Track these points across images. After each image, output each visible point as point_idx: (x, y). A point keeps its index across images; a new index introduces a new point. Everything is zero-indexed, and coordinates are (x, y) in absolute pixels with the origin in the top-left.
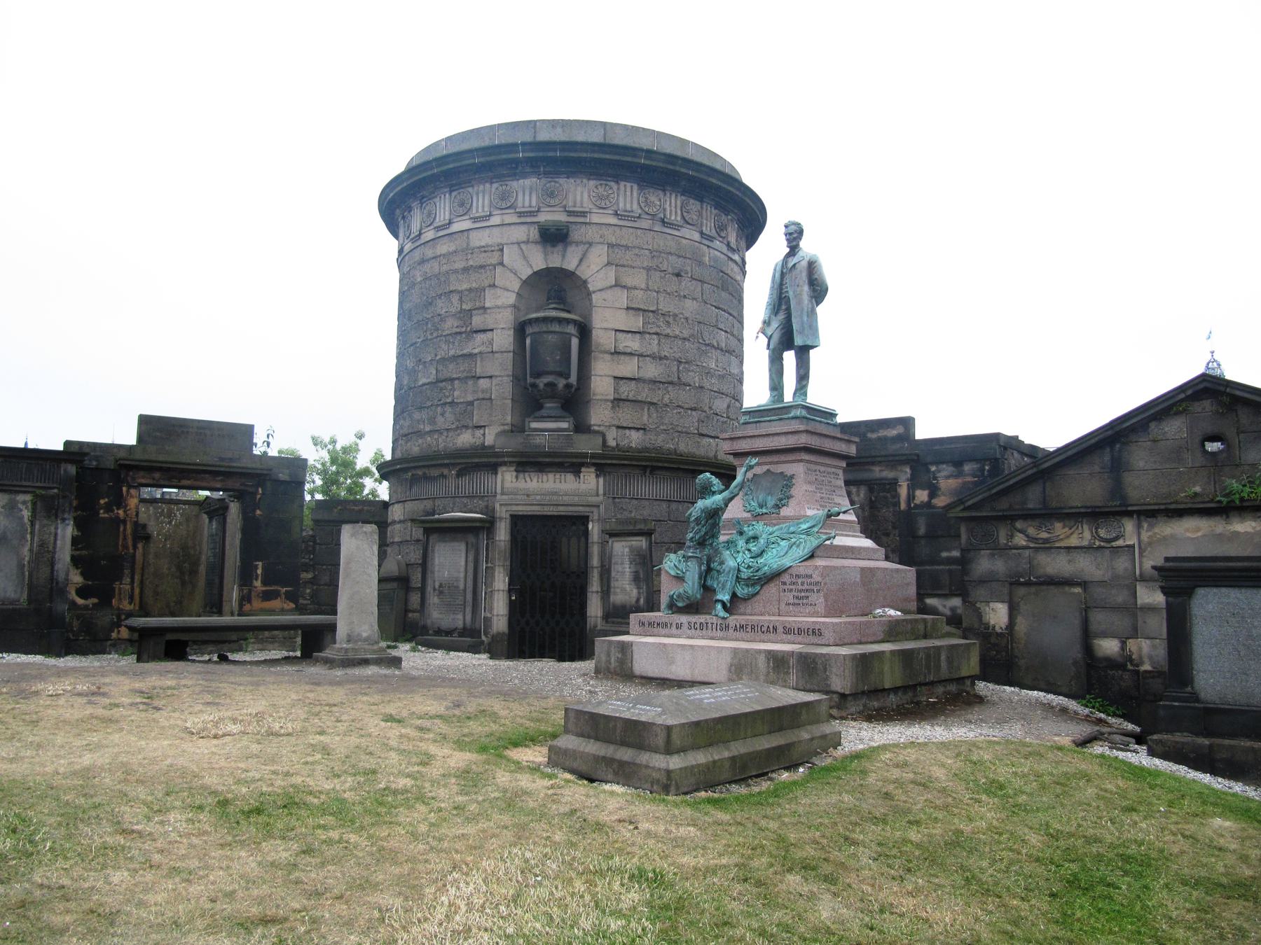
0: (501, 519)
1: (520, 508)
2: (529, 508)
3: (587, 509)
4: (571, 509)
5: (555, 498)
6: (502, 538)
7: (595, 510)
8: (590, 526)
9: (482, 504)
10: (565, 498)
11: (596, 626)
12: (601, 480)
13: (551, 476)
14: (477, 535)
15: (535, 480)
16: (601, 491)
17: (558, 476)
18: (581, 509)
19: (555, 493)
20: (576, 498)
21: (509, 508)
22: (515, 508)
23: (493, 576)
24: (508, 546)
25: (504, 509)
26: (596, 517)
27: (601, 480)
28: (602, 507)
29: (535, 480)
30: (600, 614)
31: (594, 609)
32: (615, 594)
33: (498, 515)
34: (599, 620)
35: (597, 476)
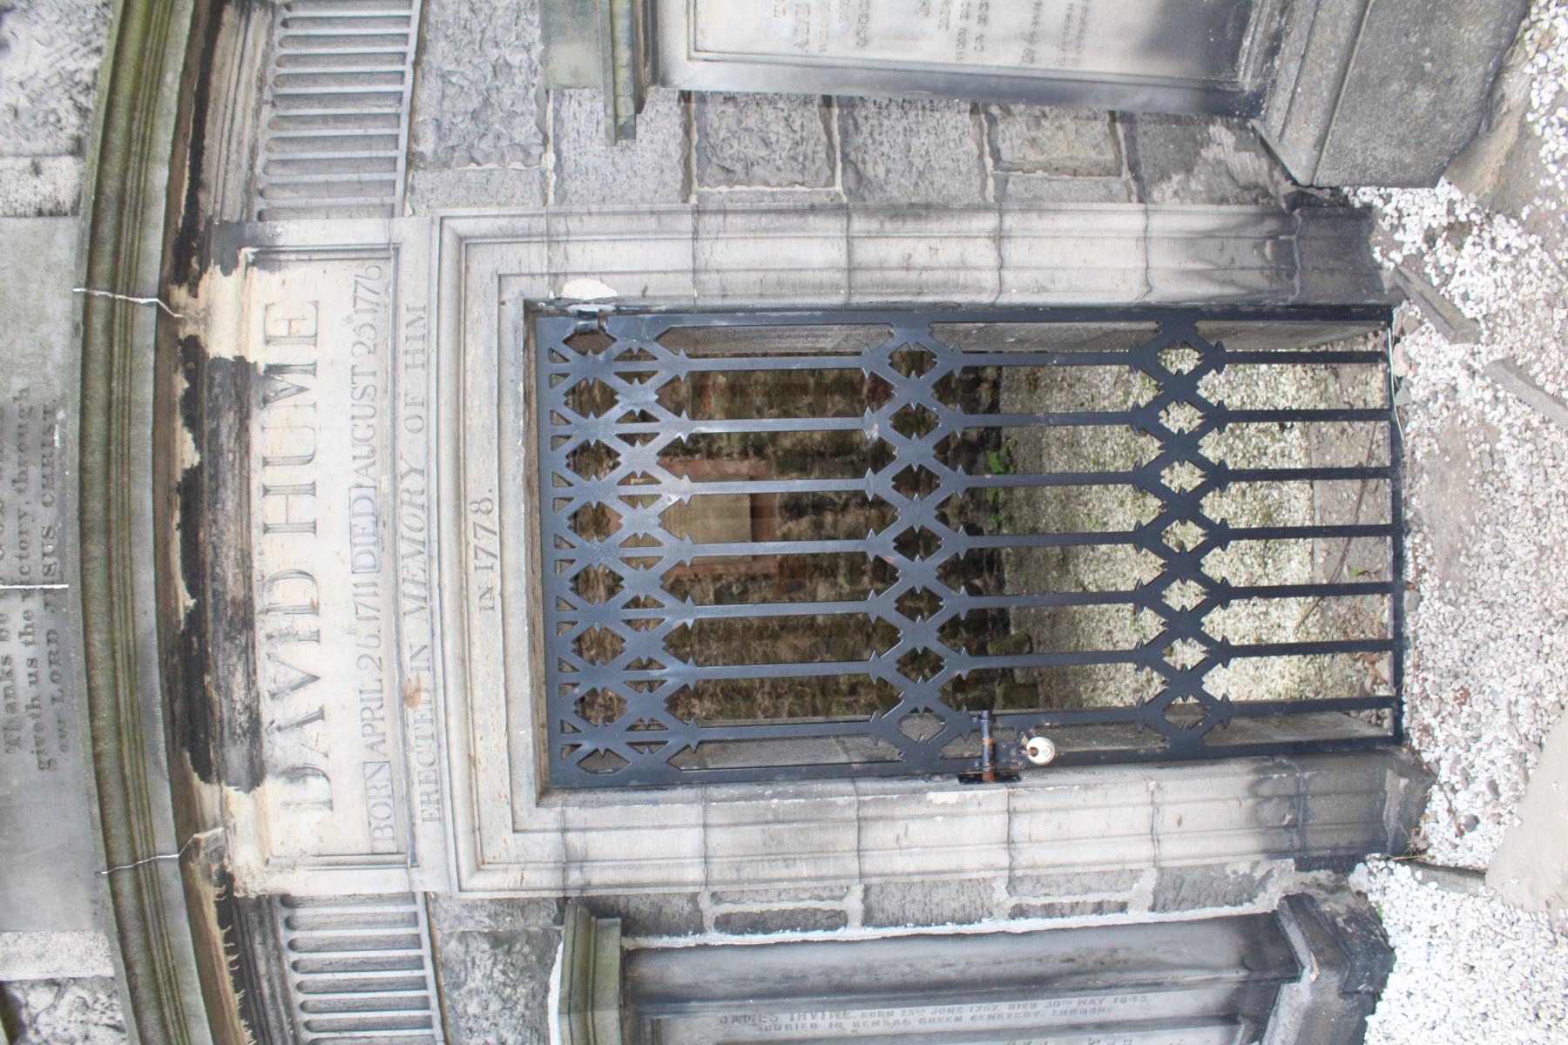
0: (568, 861)
1: (491, 746)
2: (487, 691)
3: (481, 311)
4: (480, 414)
5: (410, 519)
6: (689, 841)
7: (484, 264)
8: (585, 292)
9: (483, 971)
10: (412, 449)
11: (1192, 241)
12: (290, 232)
13: (270, 555)
14: (679, 999)
15: (304, 657)
16: (369, 230)
17: (265, 509)
18: (478, 352)
19: (385, 521)
20: (413, 383)
21: (495, 814)
22: (493, 779)
23: (932, 881)
24: (728, 802)
25: (502, 843)
26: (534, 257)
27: (290, 232)
28: (468, 221)
29: (304, 657)
30: (1127, 219)
31: (1101, 250)
32: (1076, 30)
33: (543, 881)
34: (1158, 223)
35: (268, 257)
